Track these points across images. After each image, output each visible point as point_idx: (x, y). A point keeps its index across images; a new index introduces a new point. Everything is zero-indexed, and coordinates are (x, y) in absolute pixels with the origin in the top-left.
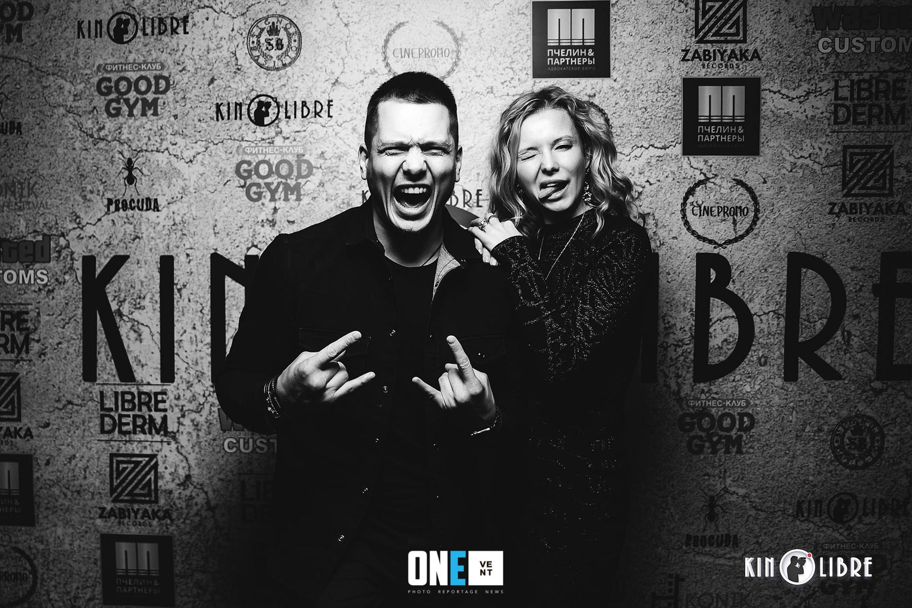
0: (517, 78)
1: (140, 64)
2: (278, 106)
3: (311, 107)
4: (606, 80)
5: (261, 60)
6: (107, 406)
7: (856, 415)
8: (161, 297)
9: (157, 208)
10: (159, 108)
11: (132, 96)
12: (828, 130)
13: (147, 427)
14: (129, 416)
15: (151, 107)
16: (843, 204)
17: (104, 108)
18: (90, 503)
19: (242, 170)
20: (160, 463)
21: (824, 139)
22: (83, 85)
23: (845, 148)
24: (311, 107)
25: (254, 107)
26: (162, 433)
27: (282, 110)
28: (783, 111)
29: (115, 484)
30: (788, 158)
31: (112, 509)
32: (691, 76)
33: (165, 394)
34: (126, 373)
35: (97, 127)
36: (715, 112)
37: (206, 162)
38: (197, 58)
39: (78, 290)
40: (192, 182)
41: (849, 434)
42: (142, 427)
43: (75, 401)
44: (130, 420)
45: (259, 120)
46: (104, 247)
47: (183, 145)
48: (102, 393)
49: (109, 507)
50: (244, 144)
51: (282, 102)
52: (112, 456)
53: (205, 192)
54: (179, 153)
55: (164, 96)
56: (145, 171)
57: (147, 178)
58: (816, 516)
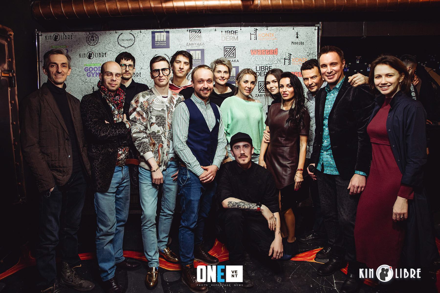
11: (93, 72)
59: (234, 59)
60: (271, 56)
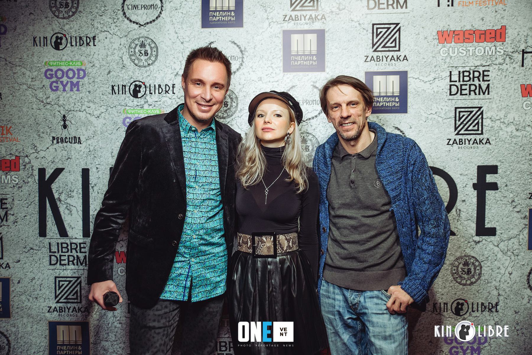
0: (274, 72)
1: (69, 62)
2: (146, 87)
3: (164, 88)
4: (323, 73)
5: (136, 62)
6: (52, 251)
7: (465, 256)
8: (83, 191)
9: (80, 142)
10: (80, 87)
11: (65, 79)
12: (446, 99)
13: (75, 261)
14: (65, 256)
15: (75, 86)
16: (455, 140)
17: (49, 86)
18: (43, 304)
19: (126, 122)
20: (83, 281)
21: (444, 104)
22: (36, 73)
23: (456, 108)
24: (164, 88)
25: (132, 87)
26: (84, 264)
27: (148, 89)
28: (420, 89)
29: (58, 293)
30: (424, 114)
31: (55, 307)
32: (369, 70)
33: (85, 243)
34: (63, 232)
35: (45, 97)
36: (383, 90)
37: (106, 117)
38: (101, 59)
39: (36, 187)
40: (99, 128)
41: (461, 266)
42: (73, 261)
43: (35, 248)
44: (66, 258)
45: (135, 94)
46: (50, 163)
47: (94, 108)
48: (50, 243)
49: (53, 307)
50: (127, 108)
51: (148, 85)
52: (56, 278)
53: (106, 134)
54: (91, 112)
55: (83, 80)
56: (73, 122)
57: (74, 126)
58: (444, 311)
59: (395, 54)
60: (487, 46)
